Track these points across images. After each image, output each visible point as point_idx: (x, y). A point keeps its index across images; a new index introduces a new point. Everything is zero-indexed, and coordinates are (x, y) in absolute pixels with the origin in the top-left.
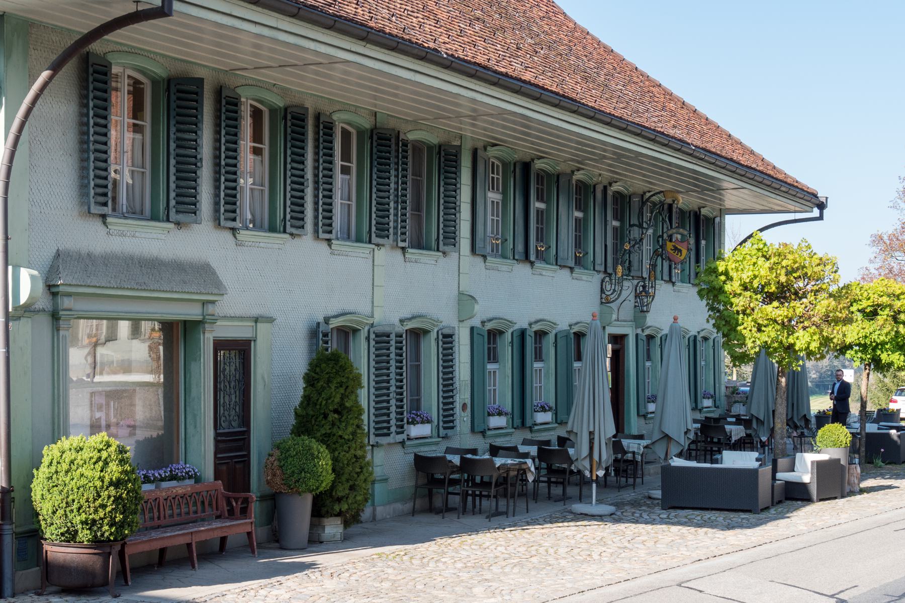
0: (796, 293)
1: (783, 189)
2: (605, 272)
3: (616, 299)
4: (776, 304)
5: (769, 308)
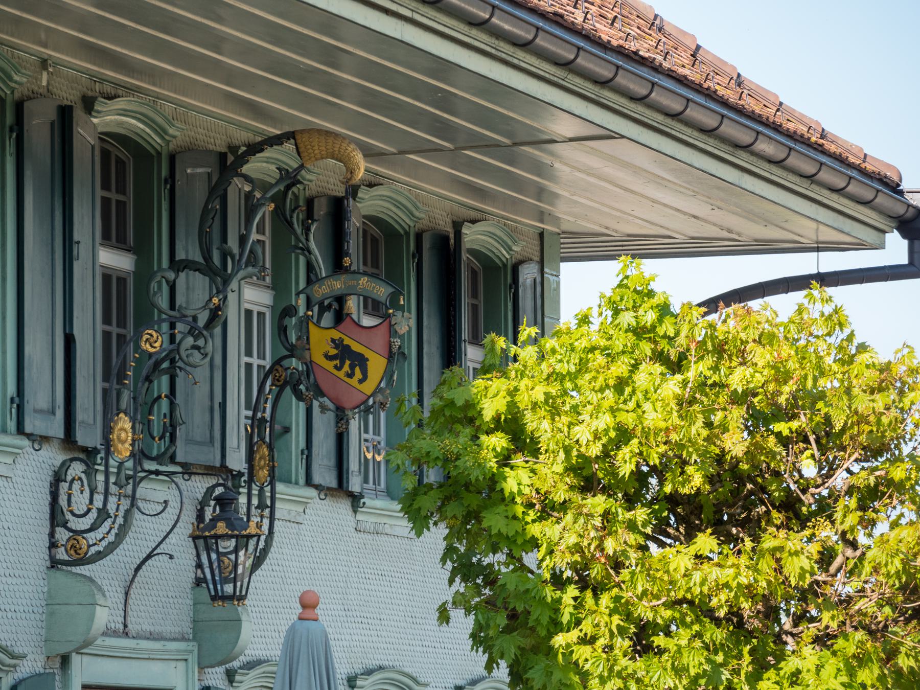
0: (790, 505)
1: (765, 147)
2: (69, 439)
3: (111, 548)
4: (705, 542)
5: (678, 558)
